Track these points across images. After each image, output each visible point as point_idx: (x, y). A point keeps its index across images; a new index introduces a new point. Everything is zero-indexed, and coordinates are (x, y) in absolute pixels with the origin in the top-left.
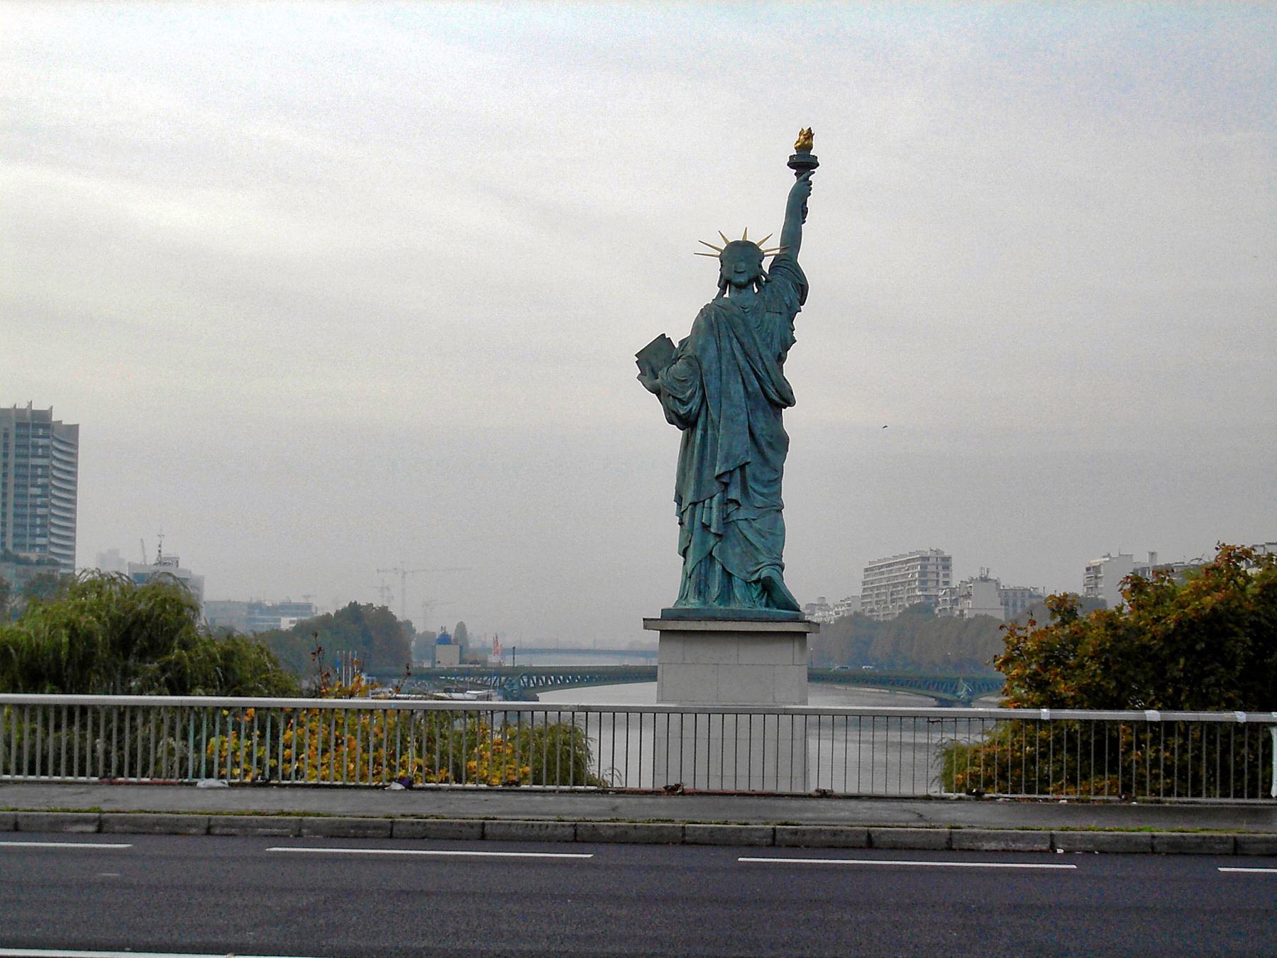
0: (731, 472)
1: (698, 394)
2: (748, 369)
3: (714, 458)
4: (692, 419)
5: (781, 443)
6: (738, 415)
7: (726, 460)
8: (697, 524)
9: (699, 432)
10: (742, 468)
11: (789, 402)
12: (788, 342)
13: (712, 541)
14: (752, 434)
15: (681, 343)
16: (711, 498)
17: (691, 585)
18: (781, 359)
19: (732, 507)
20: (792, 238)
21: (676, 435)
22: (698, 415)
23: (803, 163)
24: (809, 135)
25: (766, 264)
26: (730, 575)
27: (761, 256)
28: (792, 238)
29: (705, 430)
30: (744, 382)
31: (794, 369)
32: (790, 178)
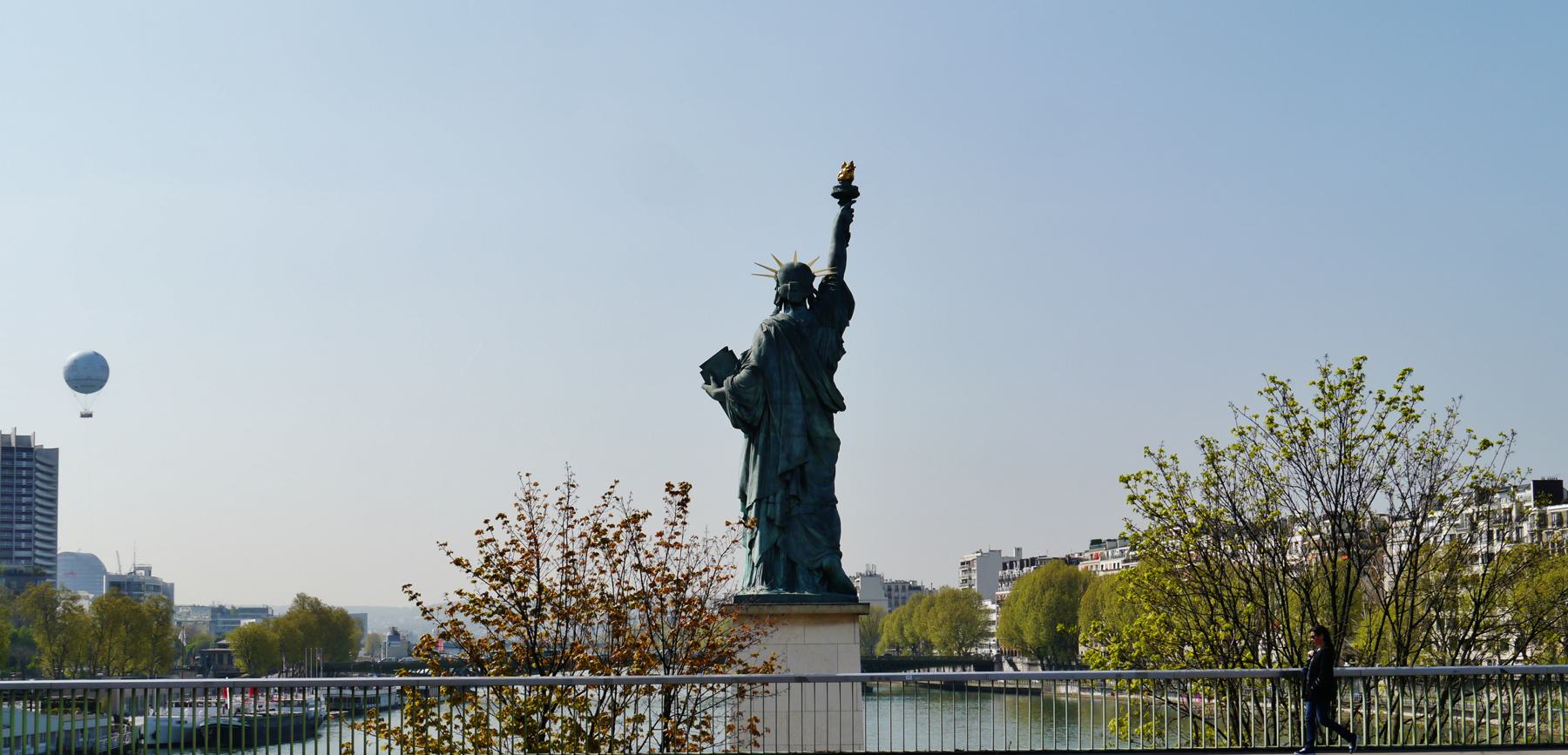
0: (792, 471)
5: (834, 443)
7: (788, 458)
8: (763, 519)
9: (762, 436)
10: (802, 467)
11: (843, 408)
13: (775, 534)
17: (758, 572)
18: (834, 369)
20: (839, 260)
23: (846, 193)
24: (852, 168)
25: (816, 284)
26: (791, 565)
28: (839, 260)
29: (768, 433)
31: (844, 378)
32: (835, 209)
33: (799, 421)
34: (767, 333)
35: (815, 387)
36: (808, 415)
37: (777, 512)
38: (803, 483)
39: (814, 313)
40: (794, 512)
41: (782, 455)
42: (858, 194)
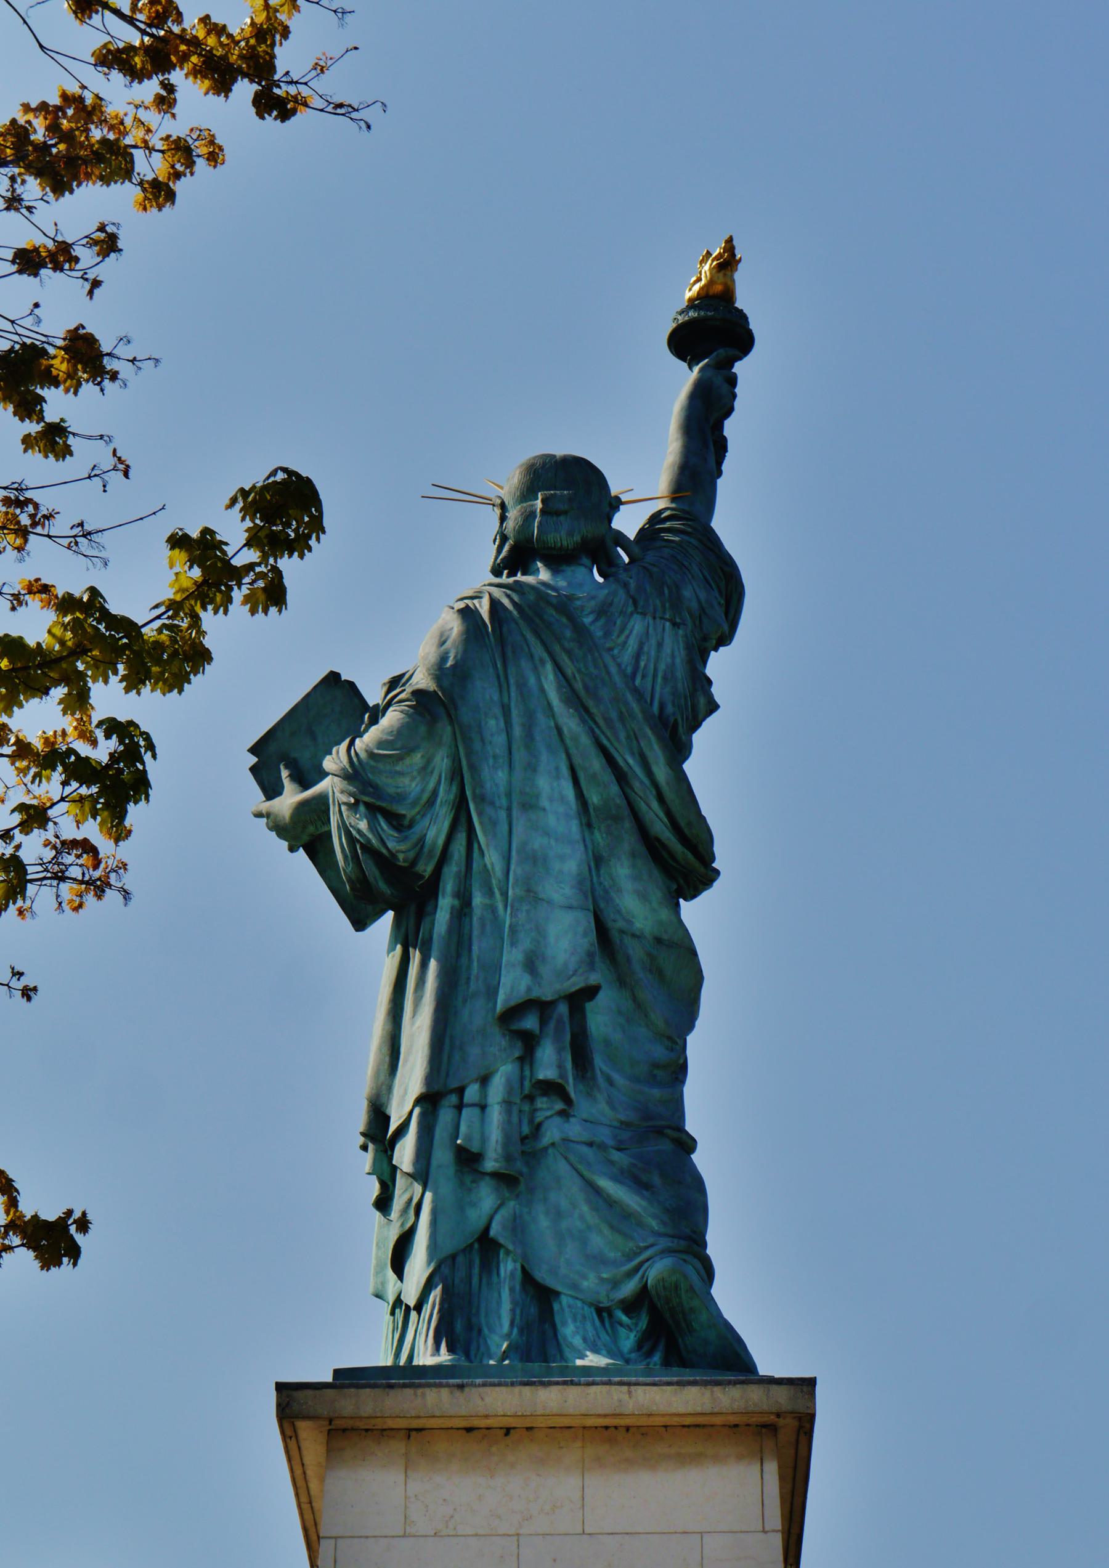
0: (542, 1007)
1: (446, 795)
2: (585, 740)
3: (494, 968)
4: (426, 868)
6: (562, 858)
7: (531, 964)
8: (442, 1156)
9: (446, 903)
13: (486, 1197)
16: (485, 1081)
19: (546, 1106)
22: (444, 857)
23: (713, 334)
26: (539, 1296)
27: (616, 504)
33: (569, 863)
34: (468, 614)
35: (621, 777)
36: (598, 861)
37: (491, 1130)
39: (614, 600)
40: (552, 1132)
41: (512, 956)
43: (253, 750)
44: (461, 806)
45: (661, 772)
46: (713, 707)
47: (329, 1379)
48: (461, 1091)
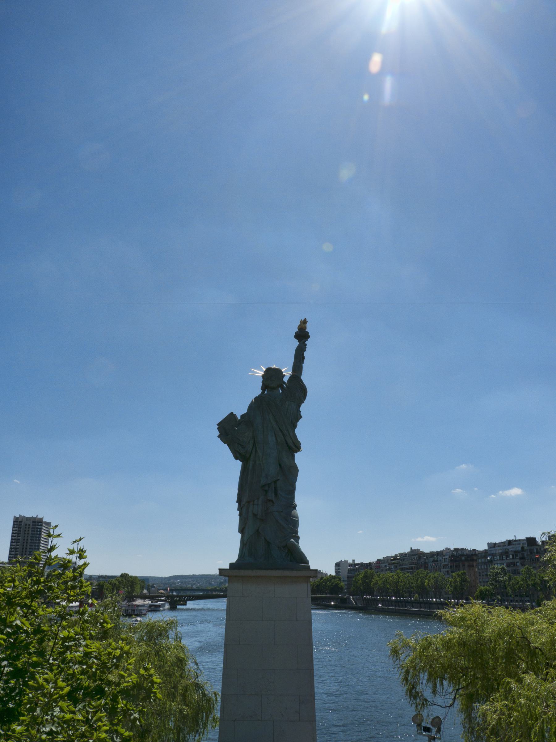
9: (251, 463)
10: (275, 482)
12: (298, 417)
14: (280, 465)
15: (242, 416)
18: (295, 426)
21: (238, 464)
23: (302, 335)
24: (304, 322)
25: (286, 380)
26: (268, 543)
30: (276, 437)
31: (302, 431)
32: (296, 343)
38: (276, 494)
42: (308, 337)
43: (218, 425)
44: (254, 443)
45: (291, 434)
46: (301, 417)
47: (227, 567)
48: (254, 501)
